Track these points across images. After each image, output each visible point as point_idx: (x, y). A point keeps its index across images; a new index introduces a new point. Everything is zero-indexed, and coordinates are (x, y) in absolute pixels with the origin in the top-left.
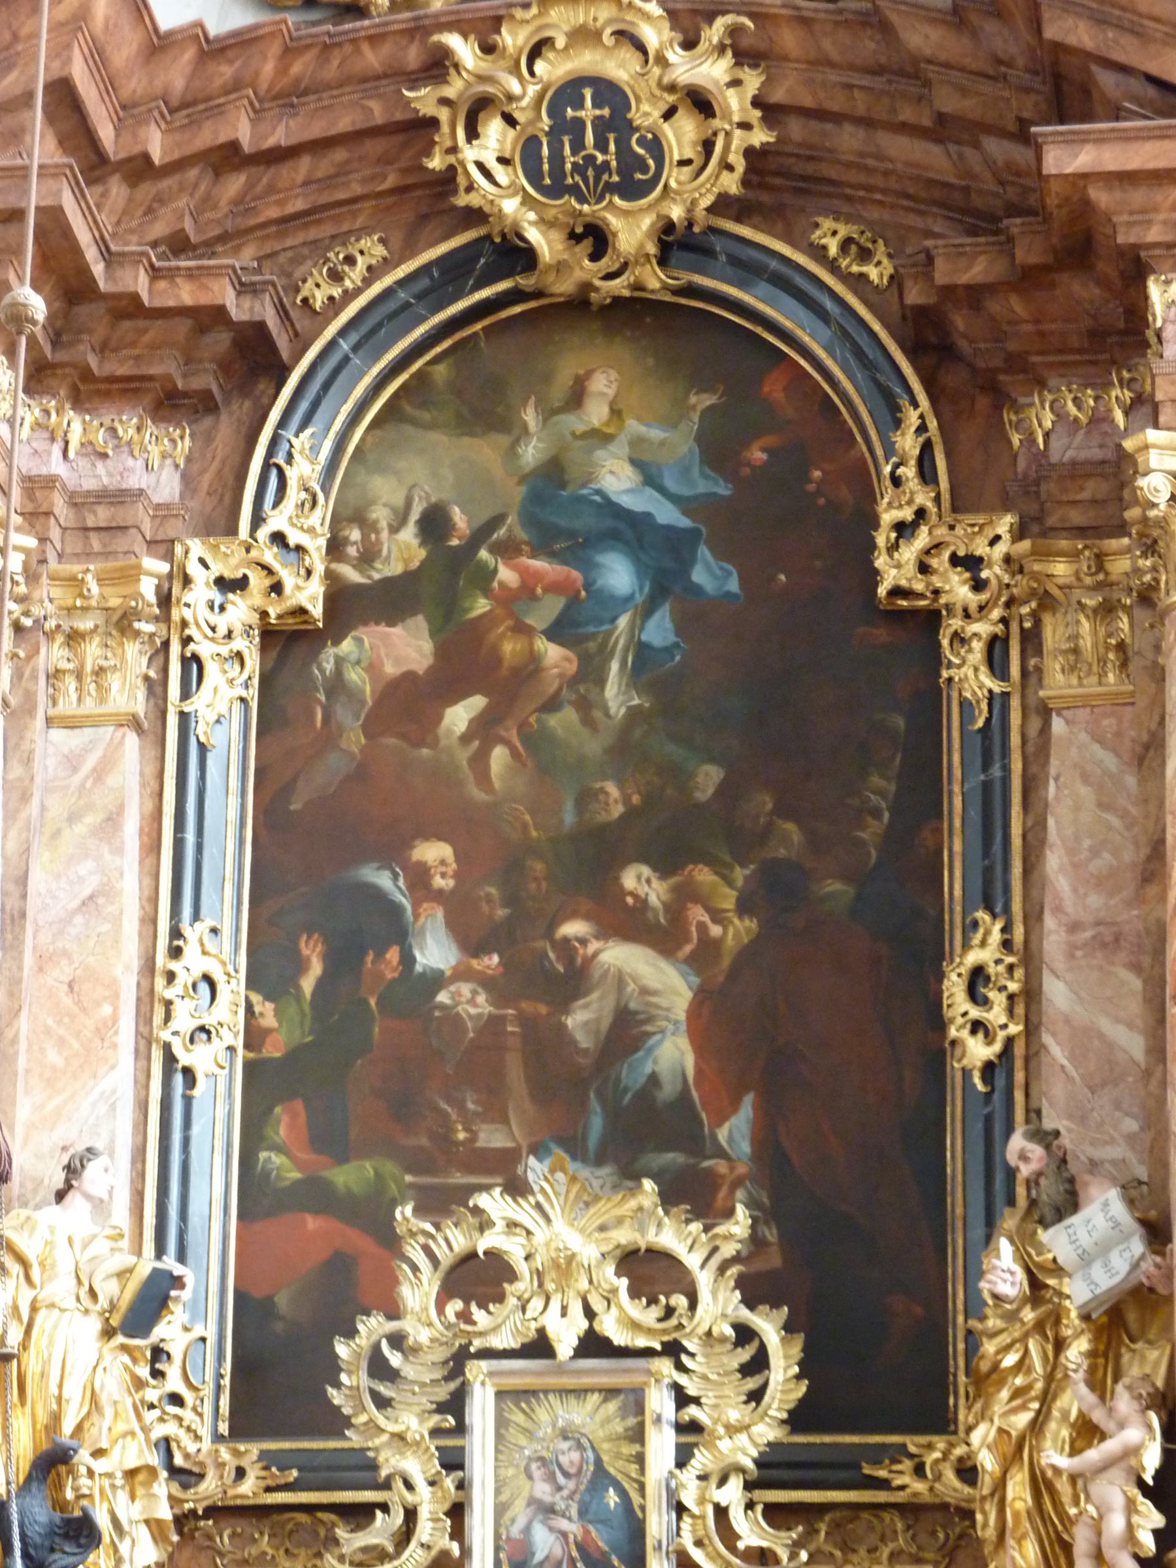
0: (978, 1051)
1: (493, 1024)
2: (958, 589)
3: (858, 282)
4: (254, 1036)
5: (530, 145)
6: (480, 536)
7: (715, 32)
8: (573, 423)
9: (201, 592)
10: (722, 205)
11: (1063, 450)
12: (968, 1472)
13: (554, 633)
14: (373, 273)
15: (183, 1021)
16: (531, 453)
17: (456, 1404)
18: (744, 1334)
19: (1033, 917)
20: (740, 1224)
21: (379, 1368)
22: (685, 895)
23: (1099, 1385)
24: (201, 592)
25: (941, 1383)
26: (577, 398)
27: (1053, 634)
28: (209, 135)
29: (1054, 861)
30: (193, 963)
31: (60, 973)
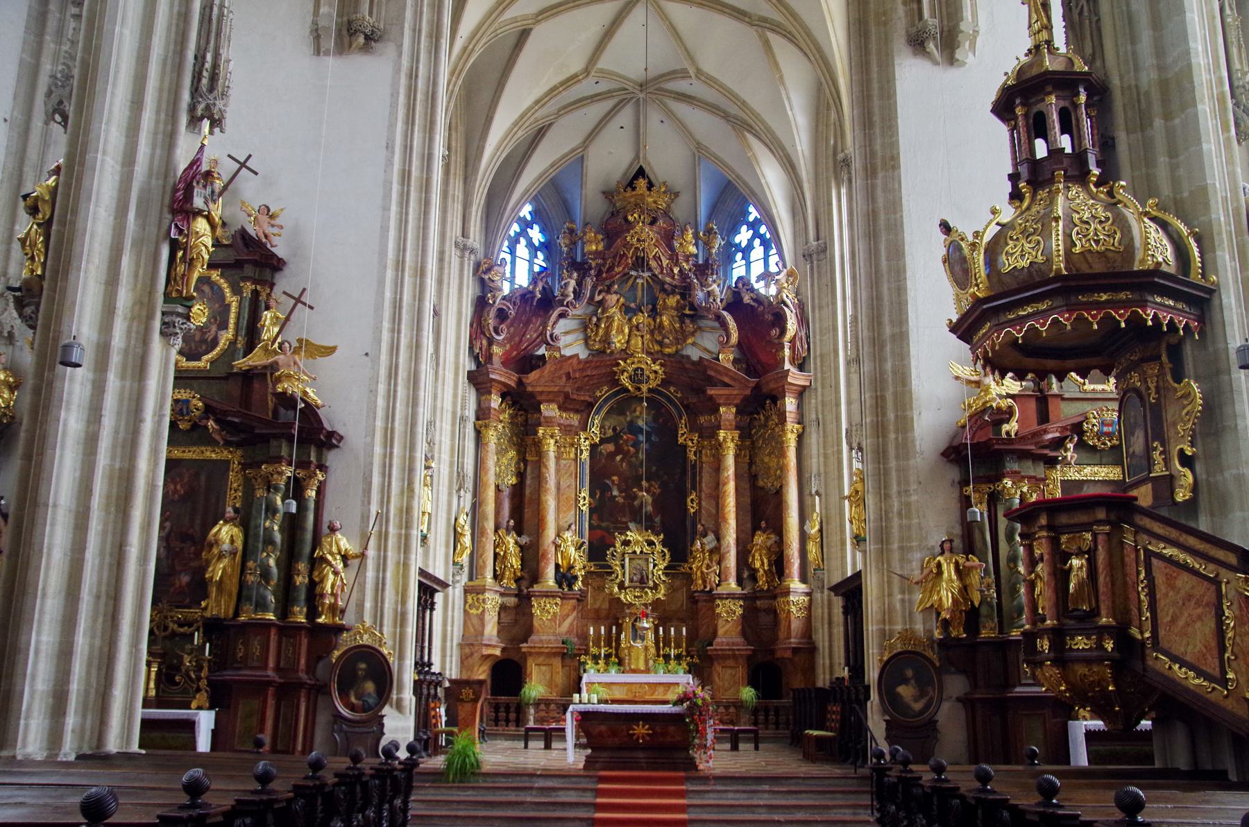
0: (692, 511)
2: (690, 443)
3: (676, 397)
4: (590, 504)
5: (630, 377)
6: (621, 431)
7: (658, 362)
8: (634, 415)
9: (582, 440)
10: (658, 385)
11: (705, 425)
12: (691, 568)
14: (606, 392)
15: (582, 503)
16: (628, 419)
17: (623, 560)
19: (700, 491)
20: (662, 536)
21: (613, 555)
22: (651, 485)
23: (711, 560)
24: (582, 440)
25: (686, 556)
27: (704, 452)
28: (585, 374)
29: (703, 485)
30: (583, 494)
31: (565, 497)
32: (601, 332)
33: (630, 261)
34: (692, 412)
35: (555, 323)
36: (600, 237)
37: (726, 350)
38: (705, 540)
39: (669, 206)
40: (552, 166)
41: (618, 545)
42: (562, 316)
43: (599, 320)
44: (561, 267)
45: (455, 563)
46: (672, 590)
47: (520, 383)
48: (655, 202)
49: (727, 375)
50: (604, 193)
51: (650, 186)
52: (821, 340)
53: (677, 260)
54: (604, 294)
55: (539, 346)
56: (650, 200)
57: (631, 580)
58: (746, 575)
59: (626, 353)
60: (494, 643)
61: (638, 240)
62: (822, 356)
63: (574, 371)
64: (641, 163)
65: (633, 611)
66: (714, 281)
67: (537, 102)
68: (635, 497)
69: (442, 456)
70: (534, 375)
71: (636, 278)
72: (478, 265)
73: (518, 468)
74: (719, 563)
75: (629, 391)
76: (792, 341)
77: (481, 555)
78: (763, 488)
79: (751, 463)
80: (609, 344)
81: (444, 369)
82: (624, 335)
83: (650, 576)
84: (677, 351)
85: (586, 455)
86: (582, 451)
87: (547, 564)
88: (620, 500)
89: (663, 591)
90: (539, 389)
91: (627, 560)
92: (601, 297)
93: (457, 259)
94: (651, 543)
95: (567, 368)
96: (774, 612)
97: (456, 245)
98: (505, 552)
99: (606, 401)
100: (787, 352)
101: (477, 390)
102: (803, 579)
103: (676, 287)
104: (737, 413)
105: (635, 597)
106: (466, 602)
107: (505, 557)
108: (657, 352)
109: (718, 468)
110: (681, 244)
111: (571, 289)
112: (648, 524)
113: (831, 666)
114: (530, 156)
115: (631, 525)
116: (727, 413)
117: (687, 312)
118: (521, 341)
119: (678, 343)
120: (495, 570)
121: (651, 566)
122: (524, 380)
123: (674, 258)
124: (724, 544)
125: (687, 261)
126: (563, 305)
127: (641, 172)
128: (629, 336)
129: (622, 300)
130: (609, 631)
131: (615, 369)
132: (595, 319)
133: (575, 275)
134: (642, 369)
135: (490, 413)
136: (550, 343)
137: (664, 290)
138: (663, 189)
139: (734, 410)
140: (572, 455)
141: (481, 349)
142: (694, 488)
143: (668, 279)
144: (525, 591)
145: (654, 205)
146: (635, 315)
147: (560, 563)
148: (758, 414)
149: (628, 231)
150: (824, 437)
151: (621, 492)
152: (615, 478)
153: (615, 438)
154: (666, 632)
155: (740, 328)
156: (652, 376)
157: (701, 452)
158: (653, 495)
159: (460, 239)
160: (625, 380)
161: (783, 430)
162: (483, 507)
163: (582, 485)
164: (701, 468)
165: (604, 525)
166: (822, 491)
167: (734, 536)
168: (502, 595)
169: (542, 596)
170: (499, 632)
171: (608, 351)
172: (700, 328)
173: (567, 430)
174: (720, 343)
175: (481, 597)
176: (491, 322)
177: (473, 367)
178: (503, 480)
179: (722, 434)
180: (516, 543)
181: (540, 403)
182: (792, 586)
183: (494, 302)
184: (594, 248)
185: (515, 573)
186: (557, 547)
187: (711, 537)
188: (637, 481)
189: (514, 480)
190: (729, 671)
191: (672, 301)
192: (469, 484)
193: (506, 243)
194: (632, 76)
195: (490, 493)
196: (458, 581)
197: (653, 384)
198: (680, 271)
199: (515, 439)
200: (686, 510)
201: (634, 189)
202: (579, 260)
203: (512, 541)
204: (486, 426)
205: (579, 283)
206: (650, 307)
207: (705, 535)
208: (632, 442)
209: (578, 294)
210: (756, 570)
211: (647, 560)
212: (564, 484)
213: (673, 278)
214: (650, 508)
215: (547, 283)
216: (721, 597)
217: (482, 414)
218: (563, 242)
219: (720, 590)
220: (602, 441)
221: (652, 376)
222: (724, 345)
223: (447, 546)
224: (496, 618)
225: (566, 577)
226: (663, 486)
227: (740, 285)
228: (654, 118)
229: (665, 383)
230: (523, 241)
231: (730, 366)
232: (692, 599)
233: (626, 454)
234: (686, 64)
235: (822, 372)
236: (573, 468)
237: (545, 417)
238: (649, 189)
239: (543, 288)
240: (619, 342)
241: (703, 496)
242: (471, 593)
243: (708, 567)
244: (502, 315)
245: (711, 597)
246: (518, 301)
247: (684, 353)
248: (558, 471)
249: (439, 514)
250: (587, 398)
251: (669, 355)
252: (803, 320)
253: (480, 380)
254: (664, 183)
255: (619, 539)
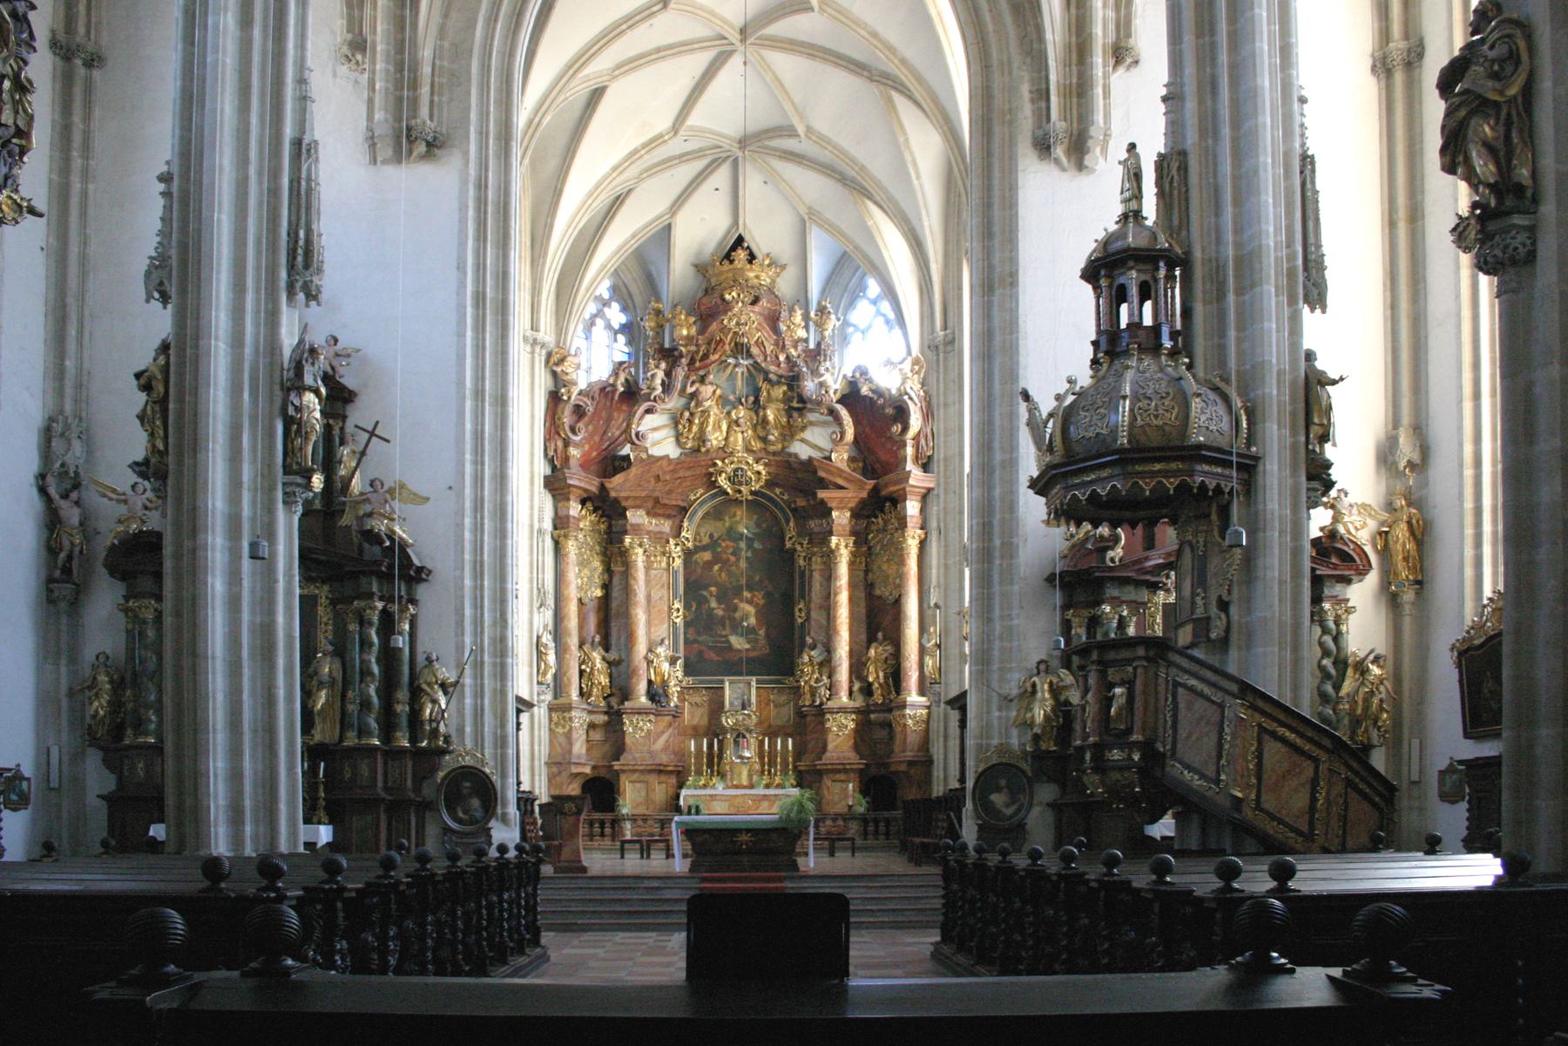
4: (685, 617)
28: (676, 476)
33: (727, 347)
34: (801, 515)
35: (641, 418)
36: (692, 319)
37: (839, 448)
42: (649, 411)
43: (692, 414)
44: (646, 355)
47: (603, 487)
48: (757, 277)
49: (841, 476)
50: (697, 266)
51: (752, 258)
52: (945, 442)
53: (784, 346)
54: (697, 385)
56: (751, 275)
59: (725, 452)
61: (738, 324)
62: (946, 459)
64: (741, 230)
70: (618, 479)
72: (549, 355)
76: (916, 438)
78: (880, 597)
79: (866, 572)
80: (704, 442)
84: (784, 448)
85: (678, 563)
90: (623, 494)
92: (693, 389)
95: (655, 470)
96: (888, 725)
98: (592, 669)
99: (701, 504)
100: (910, 451)
101: (553, 496)
102: (922, 692)
103: (781, 377)
104: (852, 516)
110: (789, 327)
111: (658, 381)
113: (946, 777)
116: (841, 518)
117: (795, 405)
120: (581, 688)
122: (608, 485)
126: (649, 400)
129: (718, 392)
130: (710, 746)
132: (687, 414)
133: (663, 365)
135: (568, 522)
138: (767, 262)
139: (848, 514)
140: (664, 565)
141: (555, 451)
142: (802, 596)
143: (773, 368)
145: (756, 281)
148: (876, 517)
149: (725, 312)
150: (946, 546)
152: (713, 589)
153: (713, 545)
154: (772, 745)
155: (856, 423)
158: (756, 606)
160: (722, 481)
161: (903, 536)
162: (566, 622)
166: (941, 603)
167: (847, 648)
168: (590, 712)
175: (567, 715)
176: (567, 418)
179: (834, 540)
180: (604, 659)
181: (625, 509)
182: (909, 699)
183: (569, 398)
186: (650, 662)
188: (738, 591)
189: (599, 593)
191: (779, 391)
192: (551, 601)
193: (581, 327)
198: (788, 358)
201: (732, 262)
202: (667, 345)
204: (566, 536)
205: (668, 374)
206: (752, 399)
208: (730, 550)
209: (667, 388)
212: (656, 595)
213: (779, 365)
215: (630, 373)
217: (561, 523)
218: (649, 324)
224: (584, 737)
226: (768, 595)
229: (770, 484)
230: (600, 322)
231: (844, 466)
233: (725, 563)
235: (946, 477)
236: (665, 578)
237: (632, 525)
239: (627, 380)
244: (579, 411)
246: (597, 396)
248: (648, 582)
251: (774, 454)
252: (928, 414)
254: (768, 255)
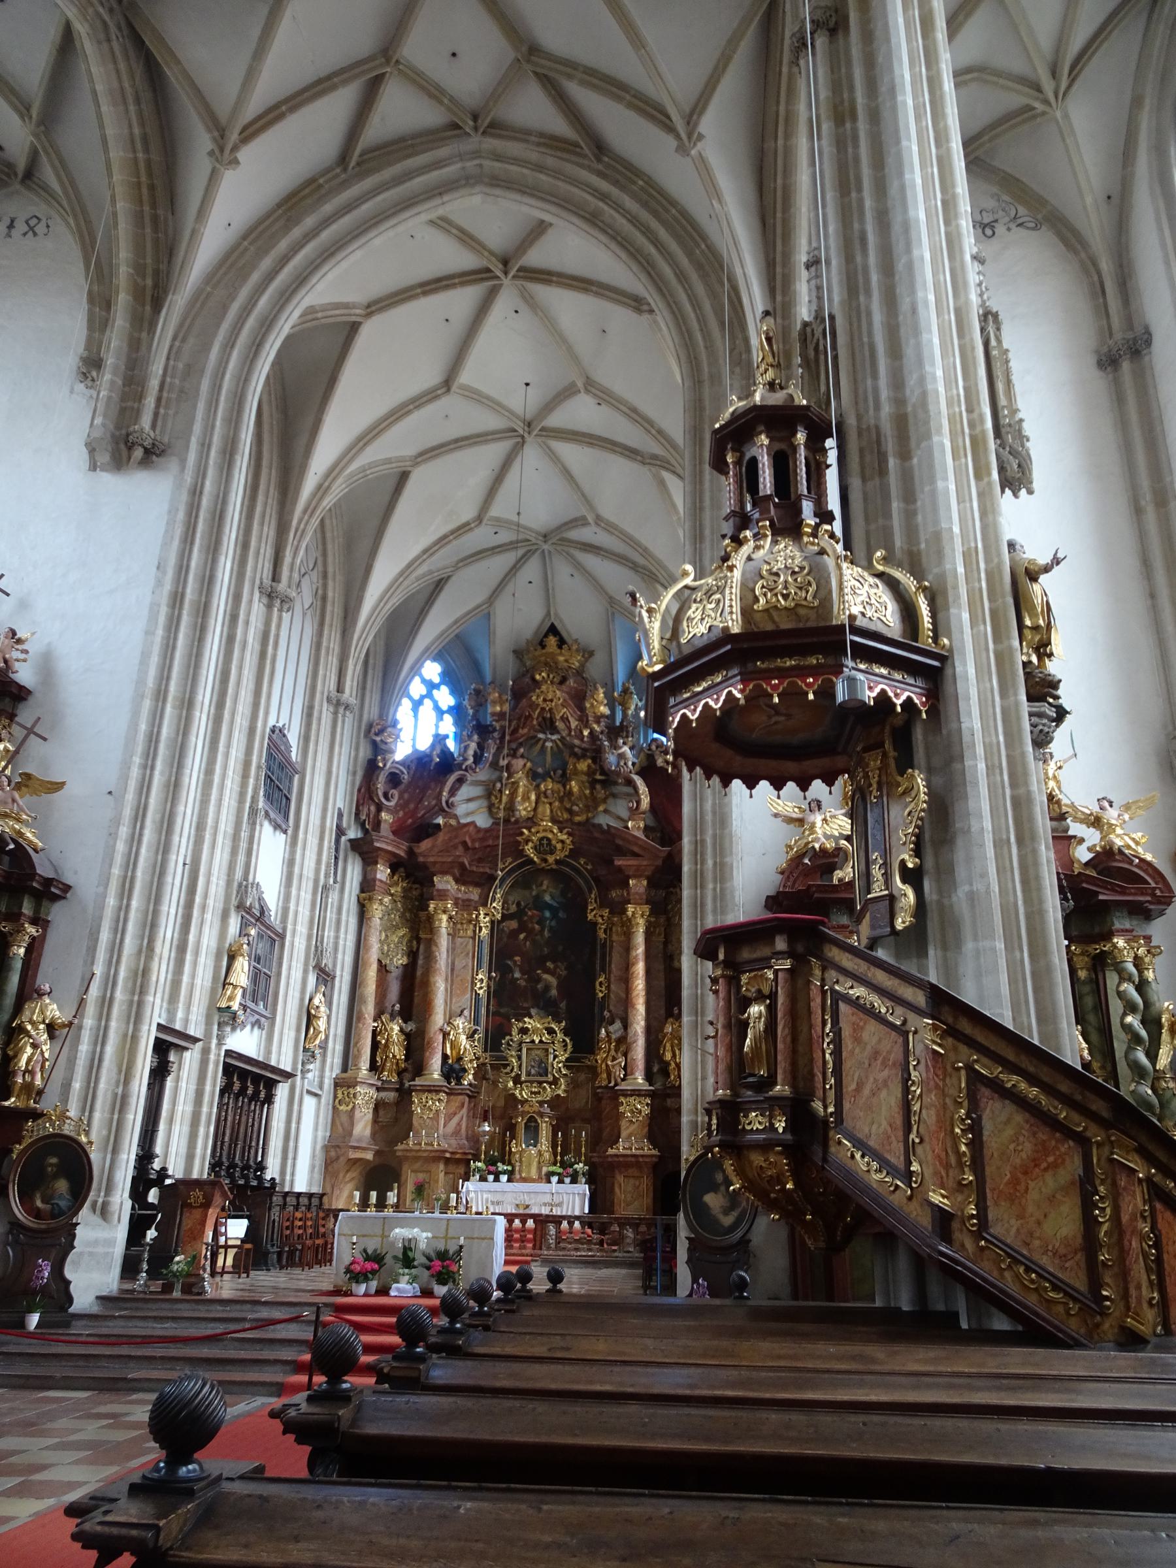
0: (601, 995)
1: (525, 987)
2: (600, 920)
3: (586, 869)
4: (489, 987)
9: (482, 916)
13: (537, 923)
16: (534, 893)
17: (520, 1050)
18: (564, 1041)
19: (610, 972)
22: (555, 968)
23: (616, 1051)
24: (482, 916)
26: (541, 884)
30: (480, 976)
32: (504, 799)
33: (535, 722)
34: (603, 887)
38: (611, 1028)
39: (583, 665)
40: (456, 622)
41: (515, 1032)
45: (305, 1050)
46: (573, 1085)
48: (566, 661)
51: (562, 642)
55: (436, 815)
56: (561, 658)
57: (528, 1074)
58: (655, 1069)
60: (364, 1145)
61: (545, 700)
63: (473, 841)
64: (553, 620)
65: (527, 1108)
66: (624, 743)
67: (425, 551)
68: (539, 980)
69: (299, 928)
71: (545, 741)
73: (409, 946)
74: (625, 1055)
75: (534, 862)
77: (356, 1043)
81: (306, 832)
82: (530, 803)
83: (550, 1069)
84: (588, 820)
86: (481, 928)
87: (432, 1054)
88: (522, 983)
89: (563, 1087)
91: (524, 1051)
92: (506, 762)
93: (330, 715)
94: (551, 1031)
97: (329, 700)
103: (585, 750)
105: (532, 1093)
106: (335, 1097)
107: (386, 1046)
108: (567, 821)
109: (628, 948)
111: (471, 752)
112: (549, 1008)
114: (428, 612)
115: (533, 1011)
117: (598, 777)
118: (416, 808)
119: (588, 811)
121: (551, 1057)
123: (584, 720)
124: (631, 1032)
125: (598, 722)
127: (553, 630)
128: (537, 803)
129: (529, 764)
131: (519, 838)
134: (549, 840)
136: (446, 810)
137: (575, 755)
140: (470, 933)
142: (603, 970)
143: (577, 742)
144: (407, 1085)
146: (544, 780)
147: (449, 1052)
149: (534, 691)
151: (523, 972)
152: (517, 958)
153: (519, 915)
156: (559, 846)
157: (611, 930)
158: (558, 978)
159: (334, 694)
160: (529, 850)
163: (479, 966)
164: (611, 947)
165: (502, 1011)
169: (424, 1091)
170: (374, 1134)
171: (513, 819)
172: (614, 796)
173: (464, 905)
174: (630, 809)
177: (360, 835)
178: (391, 960)
184: (498, 709)
185: (397, 1064)
187: (618, 1025)
189: (404, 961)
190: (632, 1181)
191: (583, 766)
194: (533, 526)
195: (372, 973)
196: (309, 1071)
197: (559, 855)
198: (591, 733)
199: (408, 915)
200: (595, 994)
203: (396, 1028)
205: (481, 747)
206: (560, 772)
207: (612, 1023)
208: (535, 920)
210: (668, 1064)
211: (547, 1050)
214: (554, 992)
216: (625, 1093)
219: (623, 1086)
220: (505, 917)
221: (559, 846)
222: (635, 812)
223: (298, 1030)
225: (452, 1071)
227: (654, 747)
228: (562, 572)
229: (574, 853)
232: (598, 1098)
234: (584, 511)
236: (470, 947)
238: (560, 647)
240: (525, 809)
241: (612, 979)
242: (342, 1087)
243: (614, 1059)
245: (615, 1095)
247: (596, 821)
248: (452, 950)
249: (290, 993)
250: (488, 870)
251: (579, 824)
253: (365, 849)
255: (516, 1026)
